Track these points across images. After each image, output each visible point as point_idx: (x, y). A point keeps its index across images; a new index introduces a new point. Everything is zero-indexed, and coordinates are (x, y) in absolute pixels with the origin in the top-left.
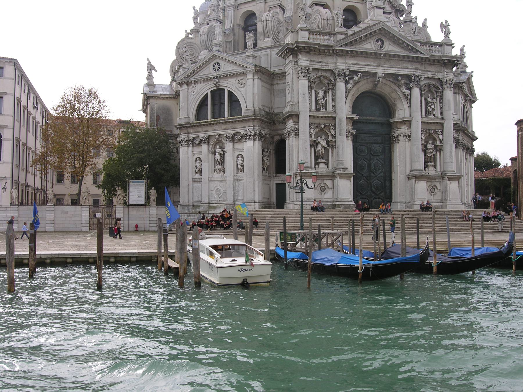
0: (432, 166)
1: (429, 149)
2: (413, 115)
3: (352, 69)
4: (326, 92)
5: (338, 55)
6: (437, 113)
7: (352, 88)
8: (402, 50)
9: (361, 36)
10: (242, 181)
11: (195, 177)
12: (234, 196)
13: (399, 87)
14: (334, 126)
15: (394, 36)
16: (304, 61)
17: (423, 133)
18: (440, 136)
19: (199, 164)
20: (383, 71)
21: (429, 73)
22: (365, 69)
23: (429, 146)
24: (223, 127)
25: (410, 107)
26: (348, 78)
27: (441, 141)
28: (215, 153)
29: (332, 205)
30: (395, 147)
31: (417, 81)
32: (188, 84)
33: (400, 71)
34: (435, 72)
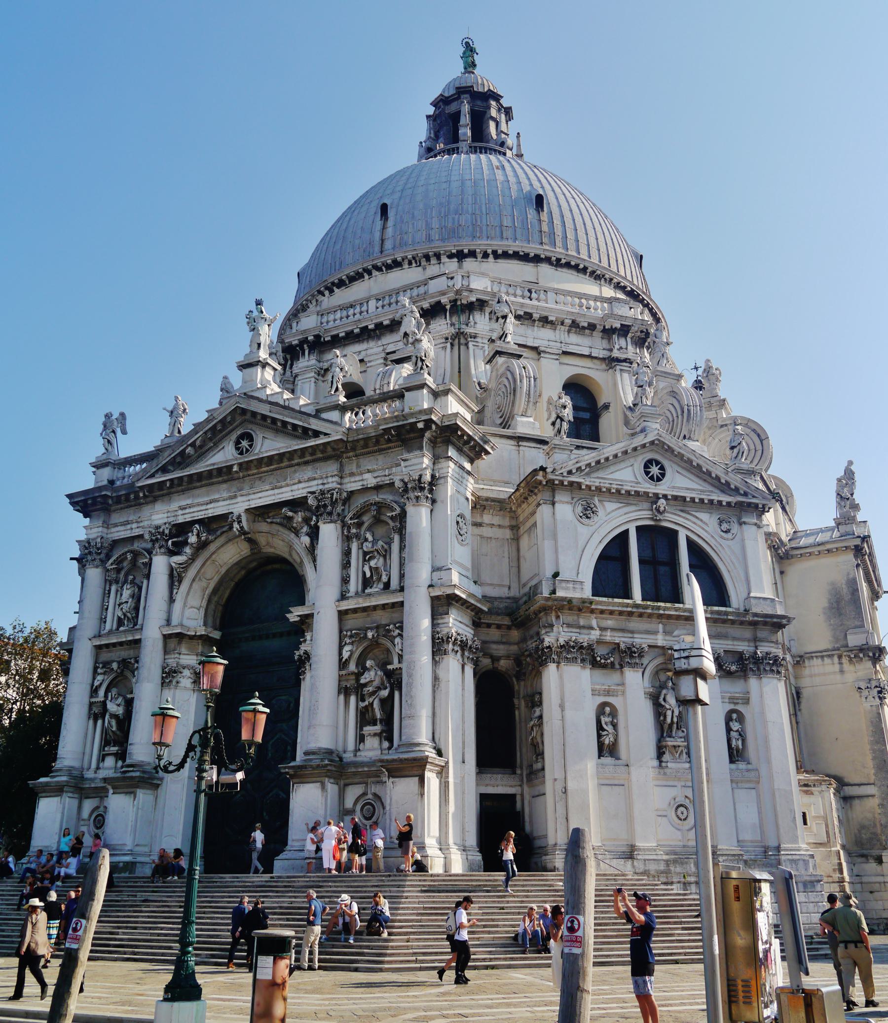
0: (375, 735)
1: (365, 685)
3: (181, 520)
7: (186, 566)
9: (189, 443)
13: (297, 533)
15: (264, 417)
17: (348, 641)
20: (246, 506)
21: (367, 476)
22: (206, 512)
26: (173, 543)
27: (400, 657)
31: (325, 506)
33: (286, 494)
34: (384, 470)
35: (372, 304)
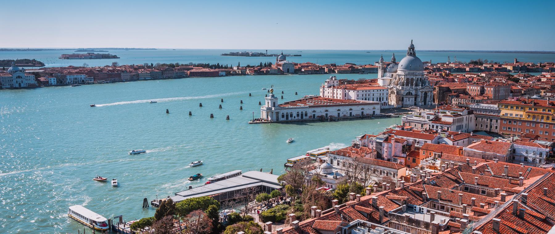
32: (405, 90)
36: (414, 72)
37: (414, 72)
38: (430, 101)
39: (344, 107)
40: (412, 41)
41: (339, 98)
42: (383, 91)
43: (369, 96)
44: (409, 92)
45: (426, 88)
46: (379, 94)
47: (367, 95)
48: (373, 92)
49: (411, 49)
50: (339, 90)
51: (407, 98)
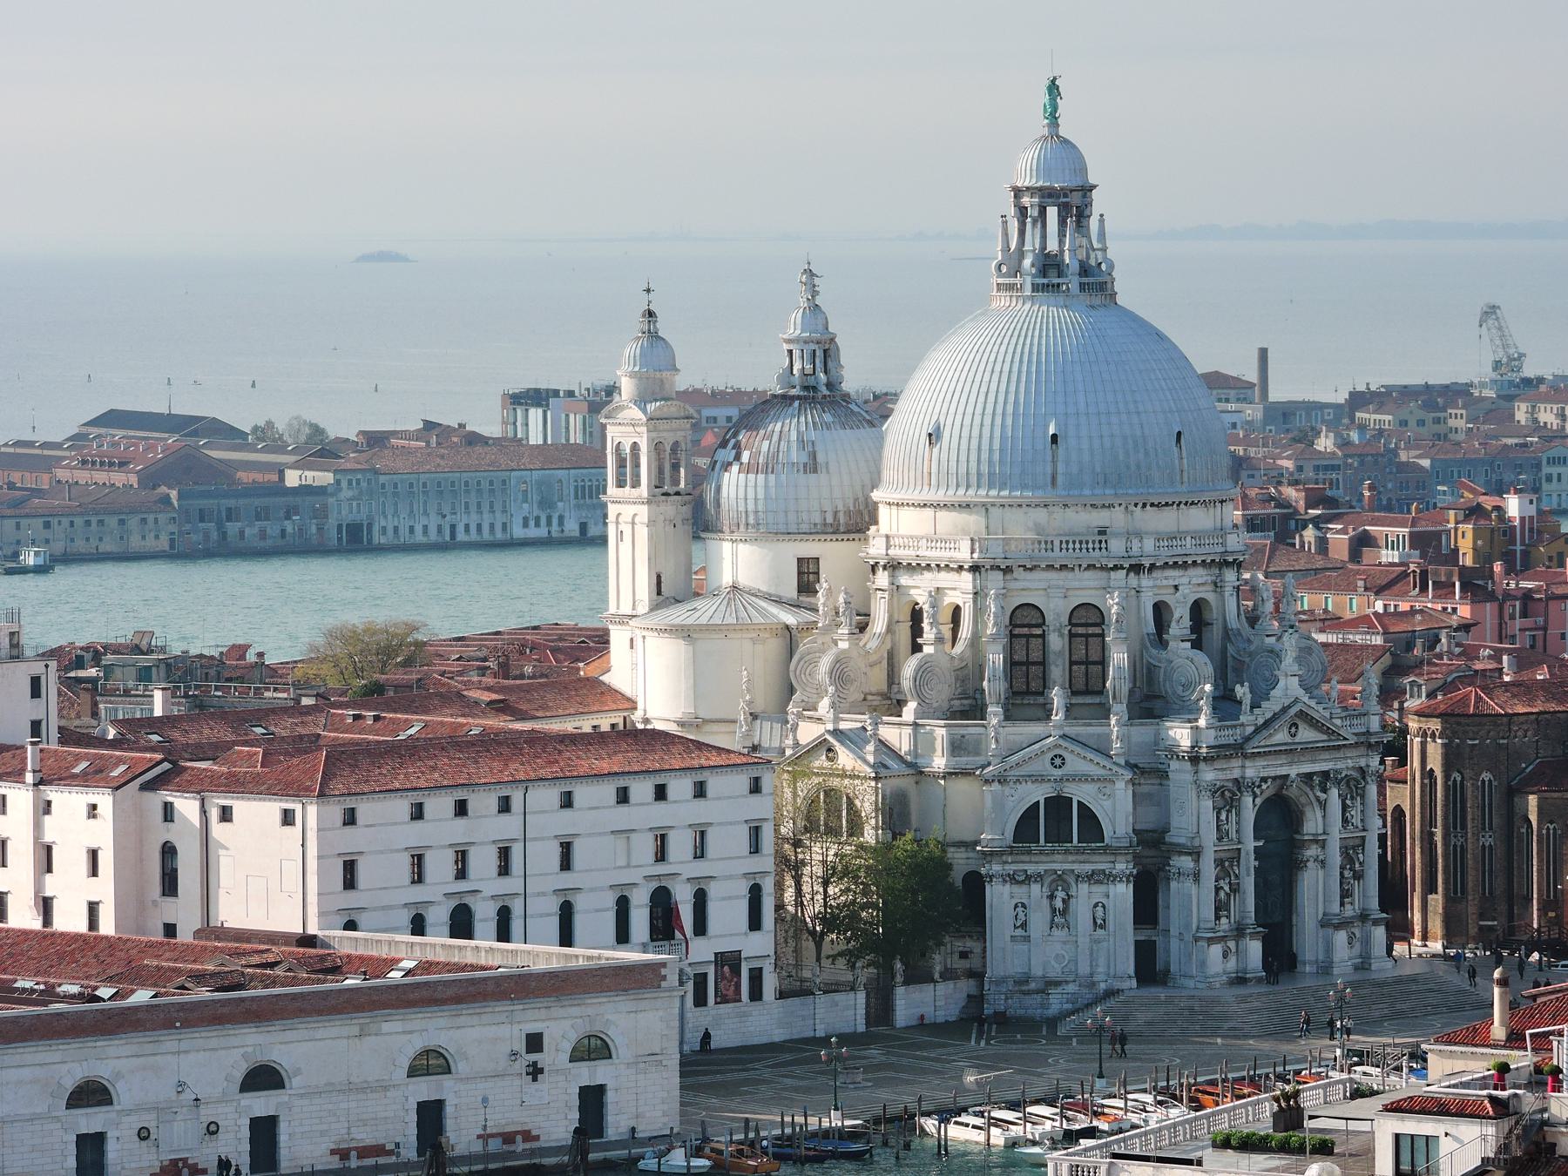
2: (1329, 830)
4: (1229, 811)
5: (1245, 756)
6: (1357, 821)
8: (1321, 735)
10: (1105, 944)
11: (1014, 934)
12: (1091, 966)
13: (1312, 788)
14: (1238, 862)
16: (1209, 775)
18: (1360, 856)
19: (1021, 915)
21: (1349, 761)
23: (1347, 874)
24: (1071, 858)
25: (1324, 817)
28: (1052, 897)
29: (1237, 977)
30: (1300, 877)
32: (1002, 780)
35: (1188, 539)
36: (1099, 518)
37: (1099, 518)
38: (1343, 924)
39: (169, 1041)
40: (1053, 88)
41: (70, 920)
42: (700, 791)
43: (504, 870)
44: (1059, 805)
45: (1281, 737)
46: (645, 847)
47: (483, 862)
48: (565, 822)
49: (1052, 213)
50: (68, 802)
51: (1028, 879)
